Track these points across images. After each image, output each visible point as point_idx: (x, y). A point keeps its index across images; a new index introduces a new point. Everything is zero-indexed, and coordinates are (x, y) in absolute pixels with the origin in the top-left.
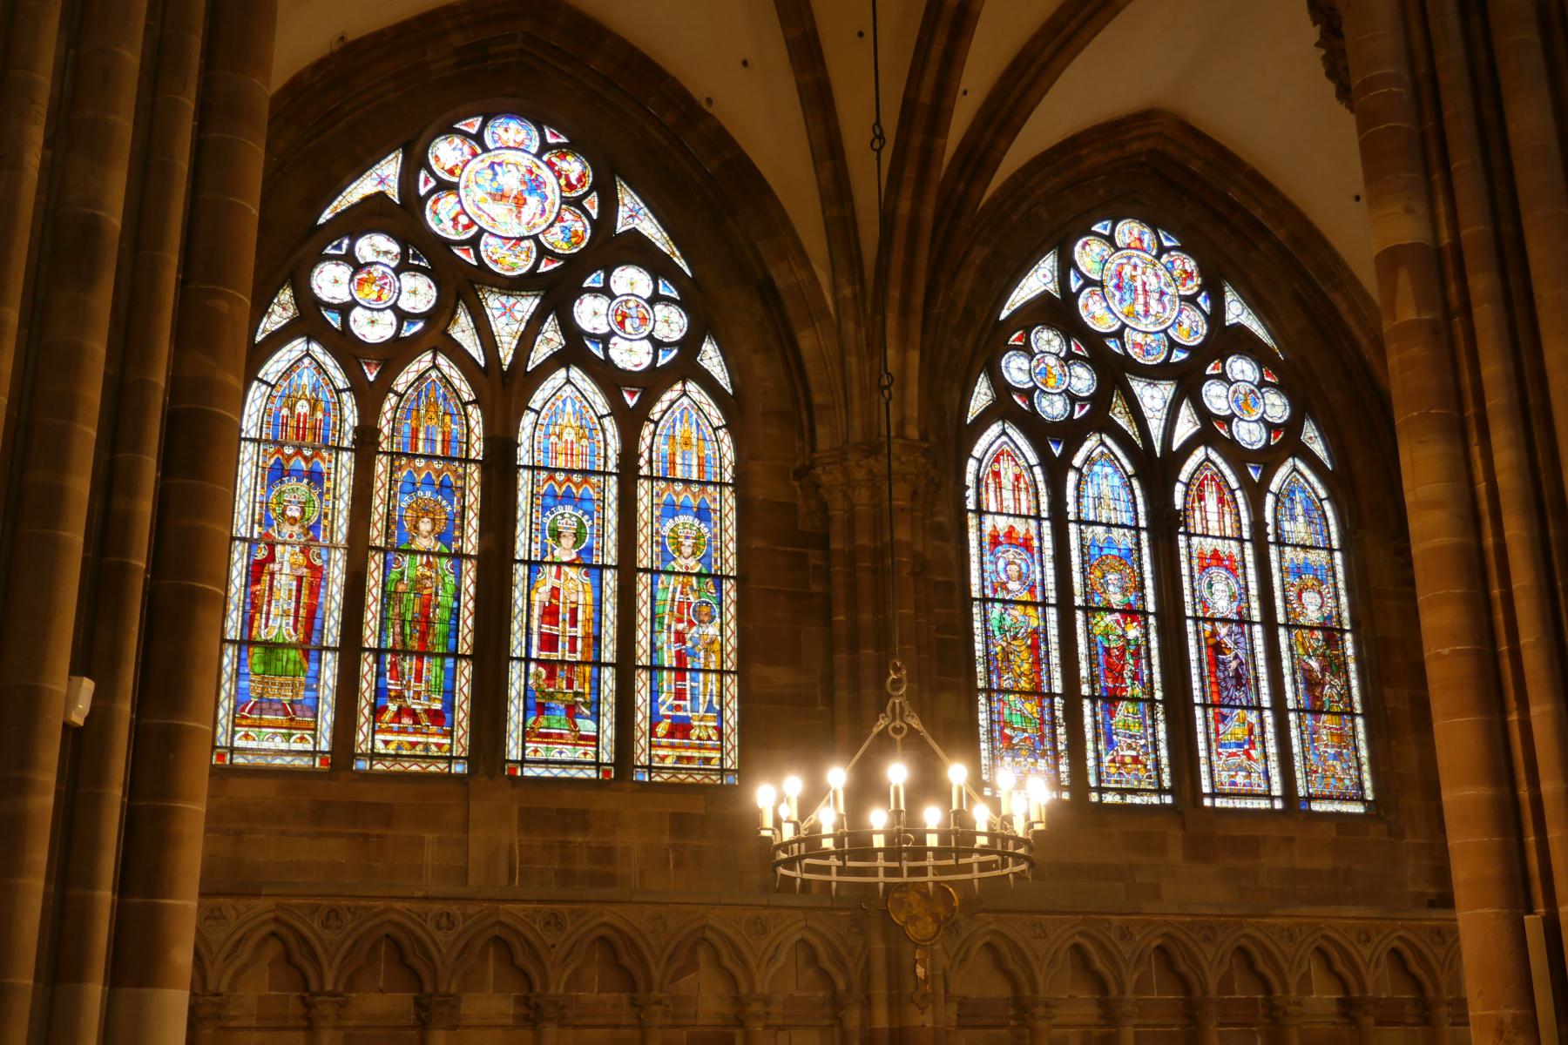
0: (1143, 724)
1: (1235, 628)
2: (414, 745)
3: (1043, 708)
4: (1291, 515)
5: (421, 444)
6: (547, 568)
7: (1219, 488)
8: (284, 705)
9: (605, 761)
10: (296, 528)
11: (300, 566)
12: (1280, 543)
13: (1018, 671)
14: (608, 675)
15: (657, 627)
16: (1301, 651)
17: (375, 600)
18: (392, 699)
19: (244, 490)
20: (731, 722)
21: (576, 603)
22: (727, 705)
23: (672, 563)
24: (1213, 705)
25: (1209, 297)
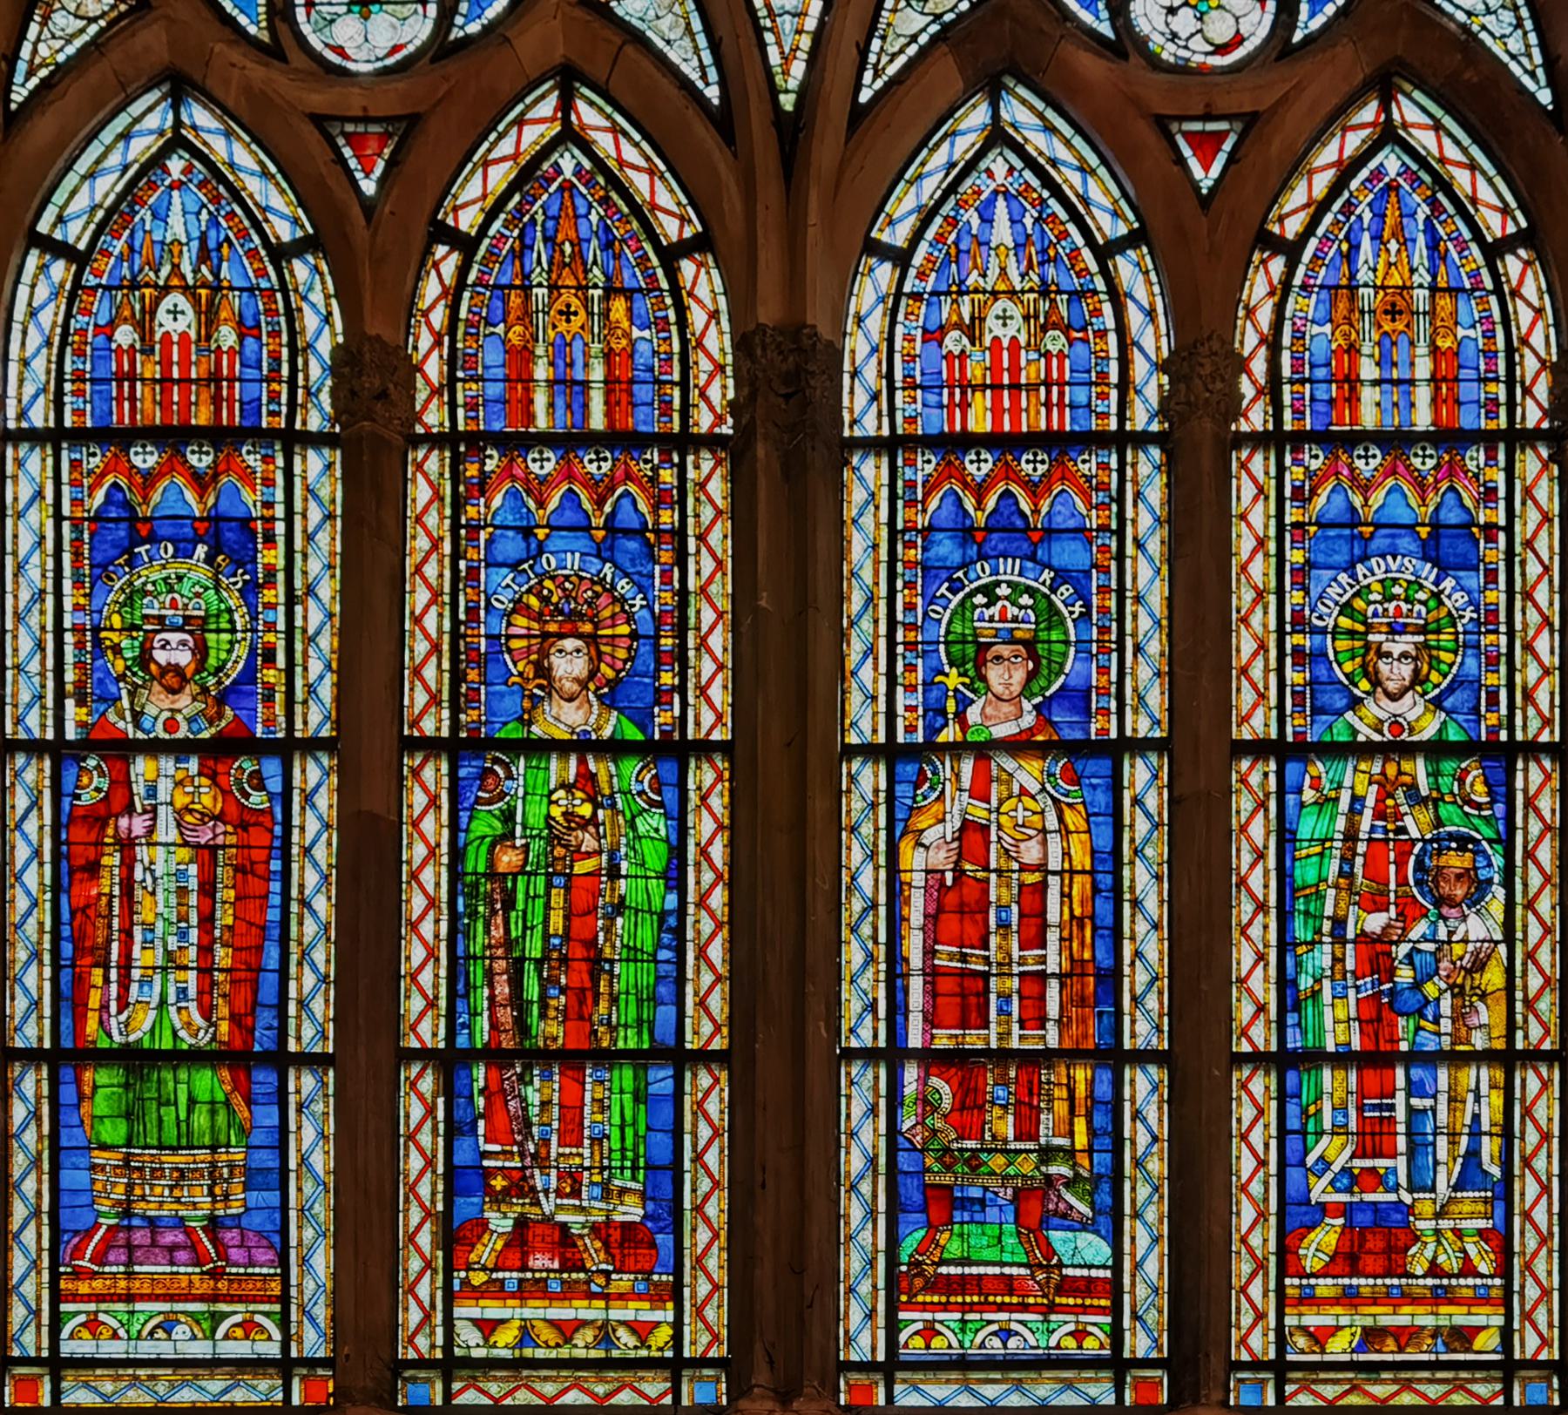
5: (540, 399)
8: (189, 1232)
9: (1140, 1354)
10: (183, 701)
11: (205, 817)
14: (1143, 1085)
15: (1301, 930)
17: (432, 903)
18: (500, 1198)
19: (25, 596)
20: (1540, 1215)
21: (1041, 867)
22: (1527, 1162)
23: (1349, 715)
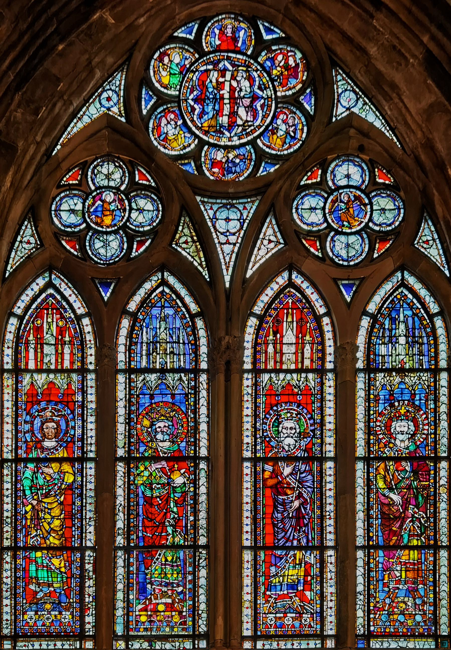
3: (71, 563)
4: (390, 337)
13: (47, 527)
16: (381, 484)
25: (315, 93)
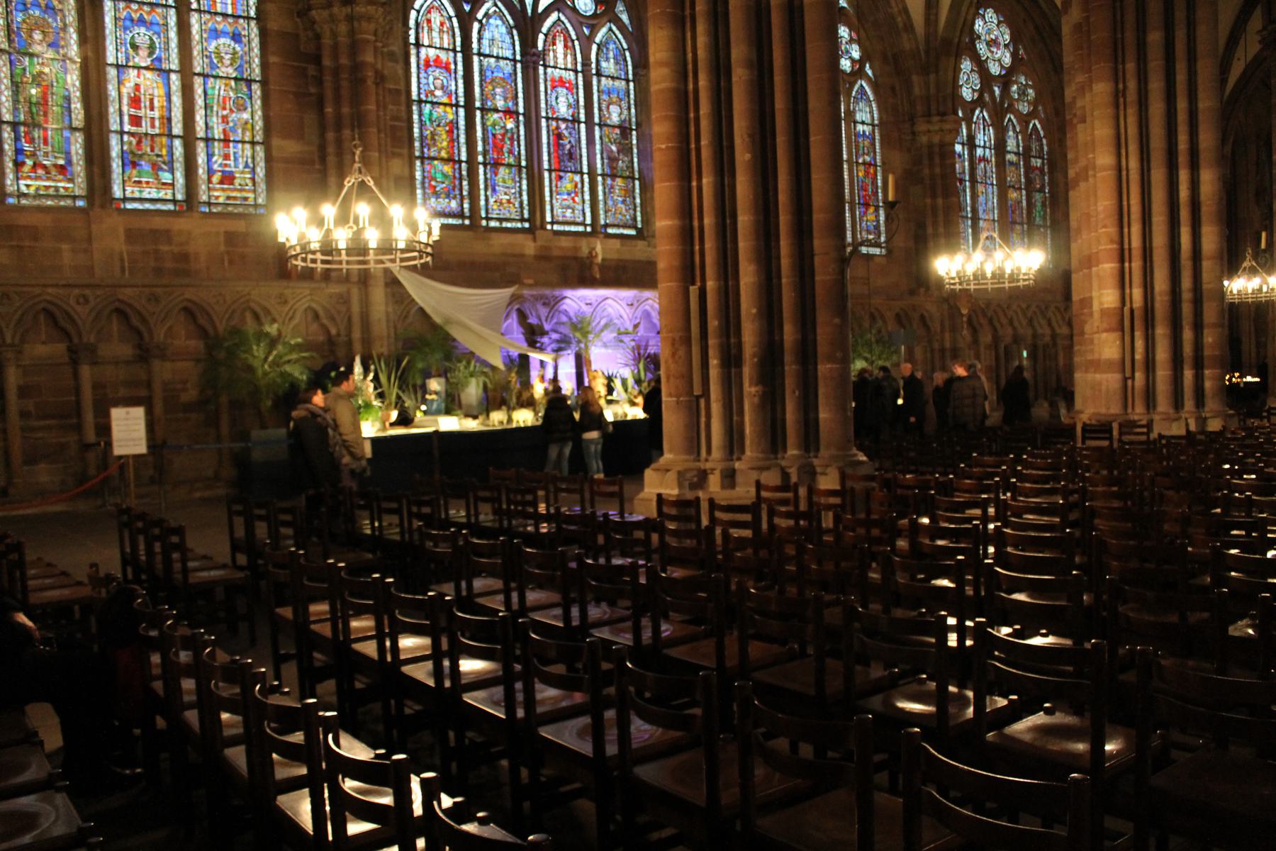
0: (513, 180)
1: (570, 125)
2: (47, 188)
6: (131, 70)
7: (565, 40)
12: (599, 74)
18: (28, 157)
21: (152, 95)
24: (555, 170)
